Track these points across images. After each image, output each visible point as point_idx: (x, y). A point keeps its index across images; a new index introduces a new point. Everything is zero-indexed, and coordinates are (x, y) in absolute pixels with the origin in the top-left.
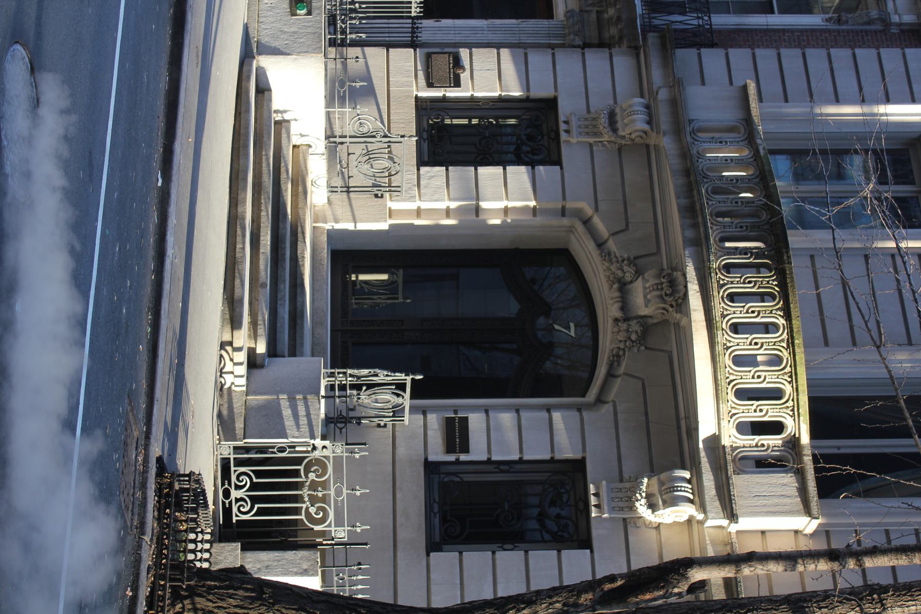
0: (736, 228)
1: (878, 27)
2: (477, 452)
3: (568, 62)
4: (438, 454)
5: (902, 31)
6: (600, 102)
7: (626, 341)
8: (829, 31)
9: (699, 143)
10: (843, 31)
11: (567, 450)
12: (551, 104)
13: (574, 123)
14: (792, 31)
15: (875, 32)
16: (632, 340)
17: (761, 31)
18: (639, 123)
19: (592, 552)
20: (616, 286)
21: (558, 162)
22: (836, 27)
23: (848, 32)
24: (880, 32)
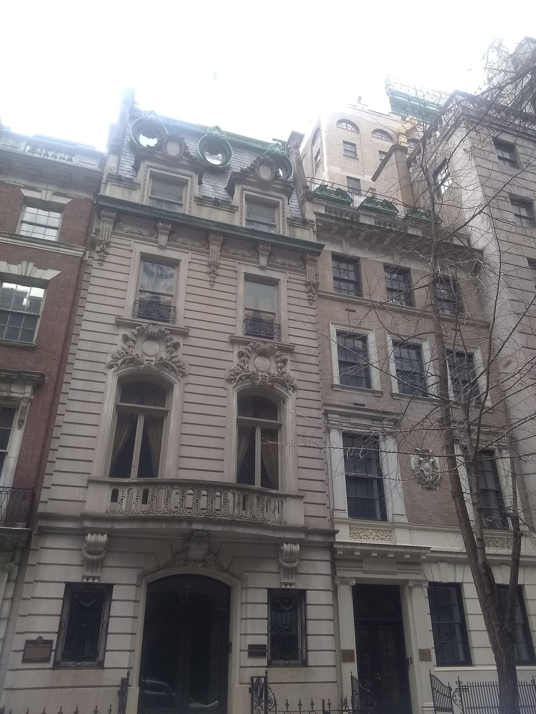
0: (183, 502)
1: (29, 404)
2: (264, 640)
3: (47, 573)
4: (264, 662)
5: (33, 394)
6: (76, 559)
7: (216, 562)
8: (25, 428)
9: (121, 510)
10: (27, 421)
11: (263, 596)
12: (69, 586)
13: (89, 574)
14: (22, 446)
15: (31, 406)
16: (217, 559)
17: (18, 462)
18: (103, 539)
19: (307, 590)
20: (188, 563)
21: (110, 587)
22: (25, 423)
23: (28, 419)
24: (31, 404)
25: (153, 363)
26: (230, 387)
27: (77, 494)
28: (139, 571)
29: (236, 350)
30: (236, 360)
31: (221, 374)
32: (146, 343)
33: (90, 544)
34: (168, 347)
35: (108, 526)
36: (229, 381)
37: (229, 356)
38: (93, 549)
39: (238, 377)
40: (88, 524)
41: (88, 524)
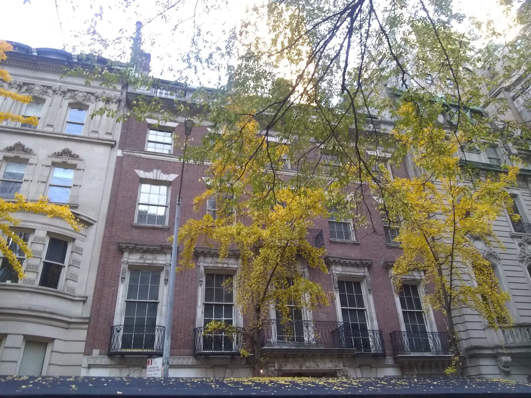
25: (485, 255)
26: (521, 264)
27: (481, 334)
28: (527, 376)
29: (517, 242)
30: (519, 249)
31: (514, 257)
32: (475, 242)
33: (505, 363)
34: (486, 244)
35: (509, 351)
36: (521, 261)
37: (513, 246)
38: (506, 365)
39: (526, 259)
40: (500, 351)
41: (500, 351)
